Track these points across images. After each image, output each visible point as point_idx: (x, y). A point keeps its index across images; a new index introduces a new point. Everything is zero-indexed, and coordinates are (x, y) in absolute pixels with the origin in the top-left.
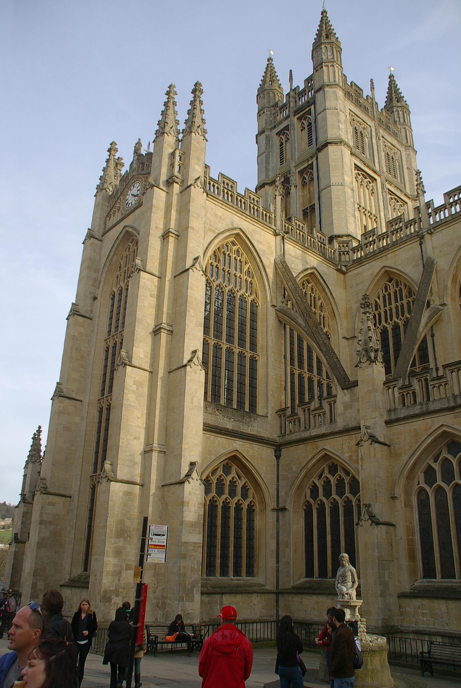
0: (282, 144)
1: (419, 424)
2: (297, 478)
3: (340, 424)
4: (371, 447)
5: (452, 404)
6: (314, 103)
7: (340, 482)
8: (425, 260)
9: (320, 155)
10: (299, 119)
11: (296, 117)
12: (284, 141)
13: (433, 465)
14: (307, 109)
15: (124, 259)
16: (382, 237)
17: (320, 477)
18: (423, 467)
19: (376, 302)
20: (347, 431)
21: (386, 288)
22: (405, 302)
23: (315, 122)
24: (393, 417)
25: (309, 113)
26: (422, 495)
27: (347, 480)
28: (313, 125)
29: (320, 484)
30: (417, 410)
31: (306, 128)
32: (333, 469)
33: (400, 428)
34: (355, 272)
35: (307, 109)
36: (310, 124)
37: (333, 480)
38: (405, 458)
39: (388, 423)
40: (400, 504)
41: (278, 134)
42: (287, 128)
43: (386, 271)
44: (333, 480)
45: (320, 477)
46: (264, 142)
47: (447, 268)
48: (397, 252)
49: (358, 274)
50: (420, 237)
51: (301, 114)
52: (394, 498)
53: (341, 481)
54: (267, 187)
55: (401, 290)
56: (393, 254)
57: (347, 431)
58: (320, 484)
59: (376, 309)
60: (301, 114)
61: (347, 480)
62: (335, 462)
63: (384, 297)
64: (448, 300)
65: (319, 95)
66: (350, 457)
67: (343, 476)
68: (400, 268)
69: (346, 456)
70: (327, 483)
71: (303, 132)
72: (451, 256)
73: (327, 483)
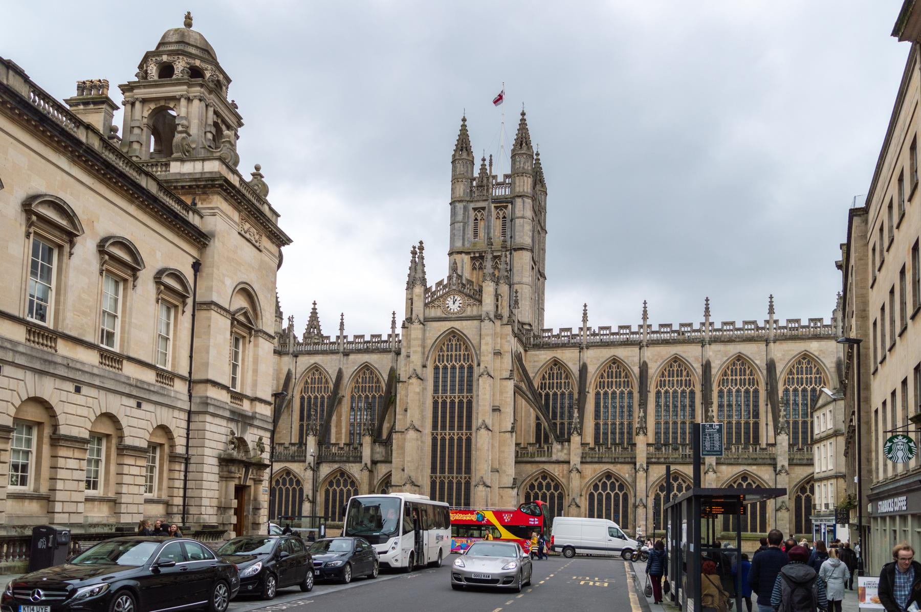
0: (476, 219)
1: (597, 466)
2: (525, 480)
3: (554, 458)
4: (577, 474)
5: (613, 461)
6: (512, 203)
7: (548, 485)
8: (581, 363)
9: (515, 253)
10: (496, 208)
11: (493, 205)
12: (479, 218)
13: (598, 483)
14: (505, 204)
15: (446, 346)
16: (558, 336)
17: (536, 480)
18: (593, 484)
19: (544, 375)
20: (558, 462)
21: (551, 368)
22: (563, 381)
23: (511, 221)
24: (584, 460)
25: (506, 207)
26: (592, 495)
27: (552, 484)
28: (508, 220)
29: (536, 484)
30: (596, 460)
31: (501, 219)
32: (544, 478)
33: (587, 466)
34: (533, 352)
35: (505, 204)
36: (504, 217)
37: (544, 483)
38: (588, 480)
39: (582, 463)
40: (583, 498)
41: (475, 209)
42: (483, 209)
43: (555, 360)
44: (544, 483)
45: (536, 480)
46: (462, 212)
47: (593, 372)
48: (564, 351)
49: (536, 355)
50: (581, 349)
51: (498, 205)
52: (581, 495)
53: (548, 485)
54: (463, 255)
55: (561, 373)
56: (561, 351)
57: (558, 462)
58: (536, 484)
59: (544, 380)
60: (498, 205)
61: (552, 484)
62: (546, 475)
63: (550, 373)
64: (591, 391)
65: (519, 201)
66: (559, 475)
67: (550, 481)
68: (565, 361)
69: (556, 474)
70: (540, 484)
71: (498, 220)
72: (597, 367)
73: (540, 484)
